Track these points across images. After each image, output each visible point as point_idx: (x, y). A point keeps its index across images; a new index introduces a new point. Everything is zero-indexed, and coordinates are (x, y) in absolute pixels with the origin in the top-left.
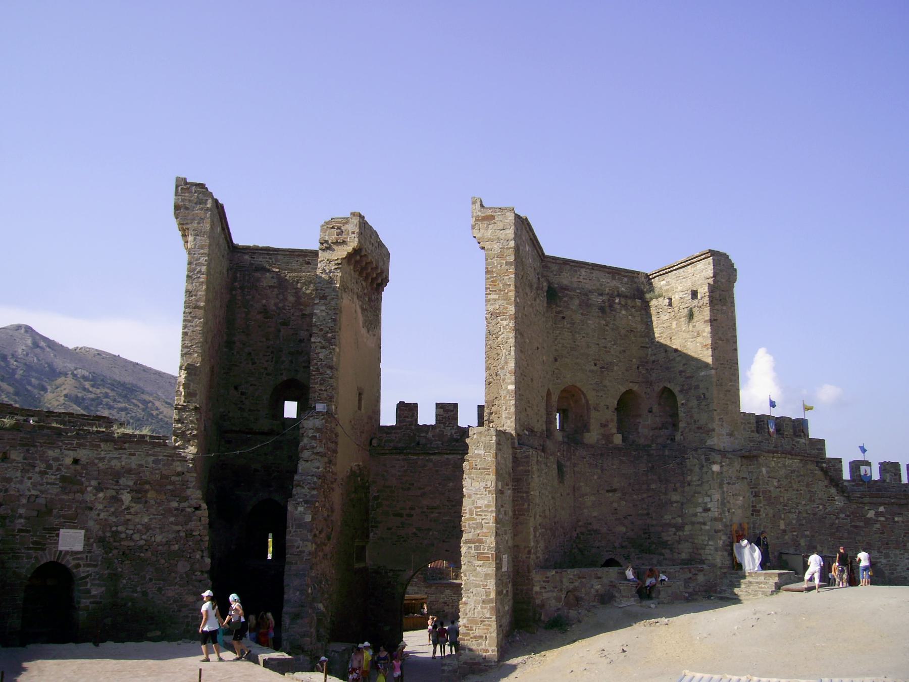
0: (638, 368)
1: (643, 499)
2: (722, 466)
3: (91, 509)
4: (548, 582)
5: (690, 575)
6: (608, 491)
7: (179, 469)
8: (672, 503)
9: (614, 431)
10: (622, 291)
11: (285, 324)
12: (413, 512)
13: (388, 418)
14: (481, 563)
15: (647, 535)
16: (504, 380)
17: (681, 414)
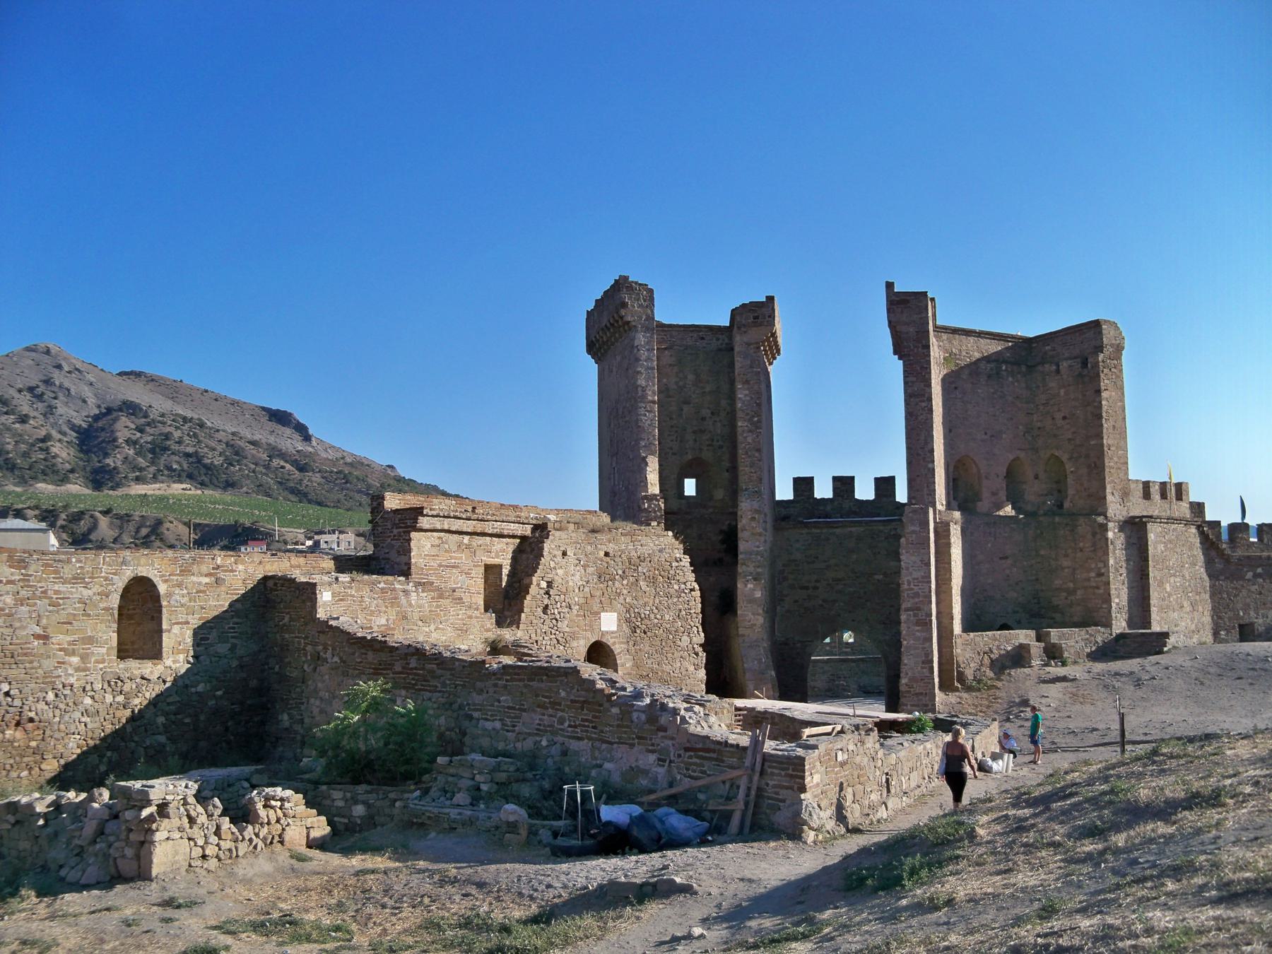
0: (1024, 435)
1: (1032, 565)
2: (1114, 533)
3: (619, 594)
4: (967, 644)
5: (1088, 636)
6: (1001, 558)
7: (678, 555)
8: (1063, 569)
9: (1005, 498)
10: (1008, 357)
11: (687, 402)
12: (818, 584)
13: (784, 492)
14: (918, 628)
15: (1036, 601)
16: (924, 458)
17: (1070, 481)
